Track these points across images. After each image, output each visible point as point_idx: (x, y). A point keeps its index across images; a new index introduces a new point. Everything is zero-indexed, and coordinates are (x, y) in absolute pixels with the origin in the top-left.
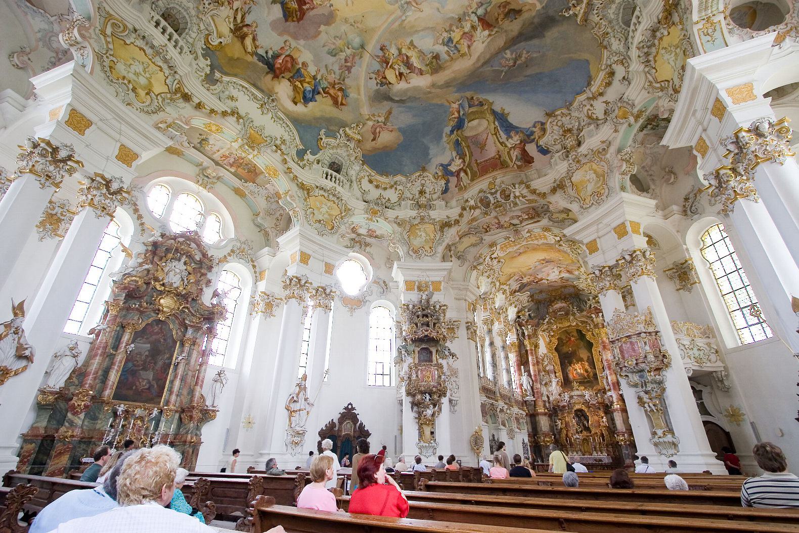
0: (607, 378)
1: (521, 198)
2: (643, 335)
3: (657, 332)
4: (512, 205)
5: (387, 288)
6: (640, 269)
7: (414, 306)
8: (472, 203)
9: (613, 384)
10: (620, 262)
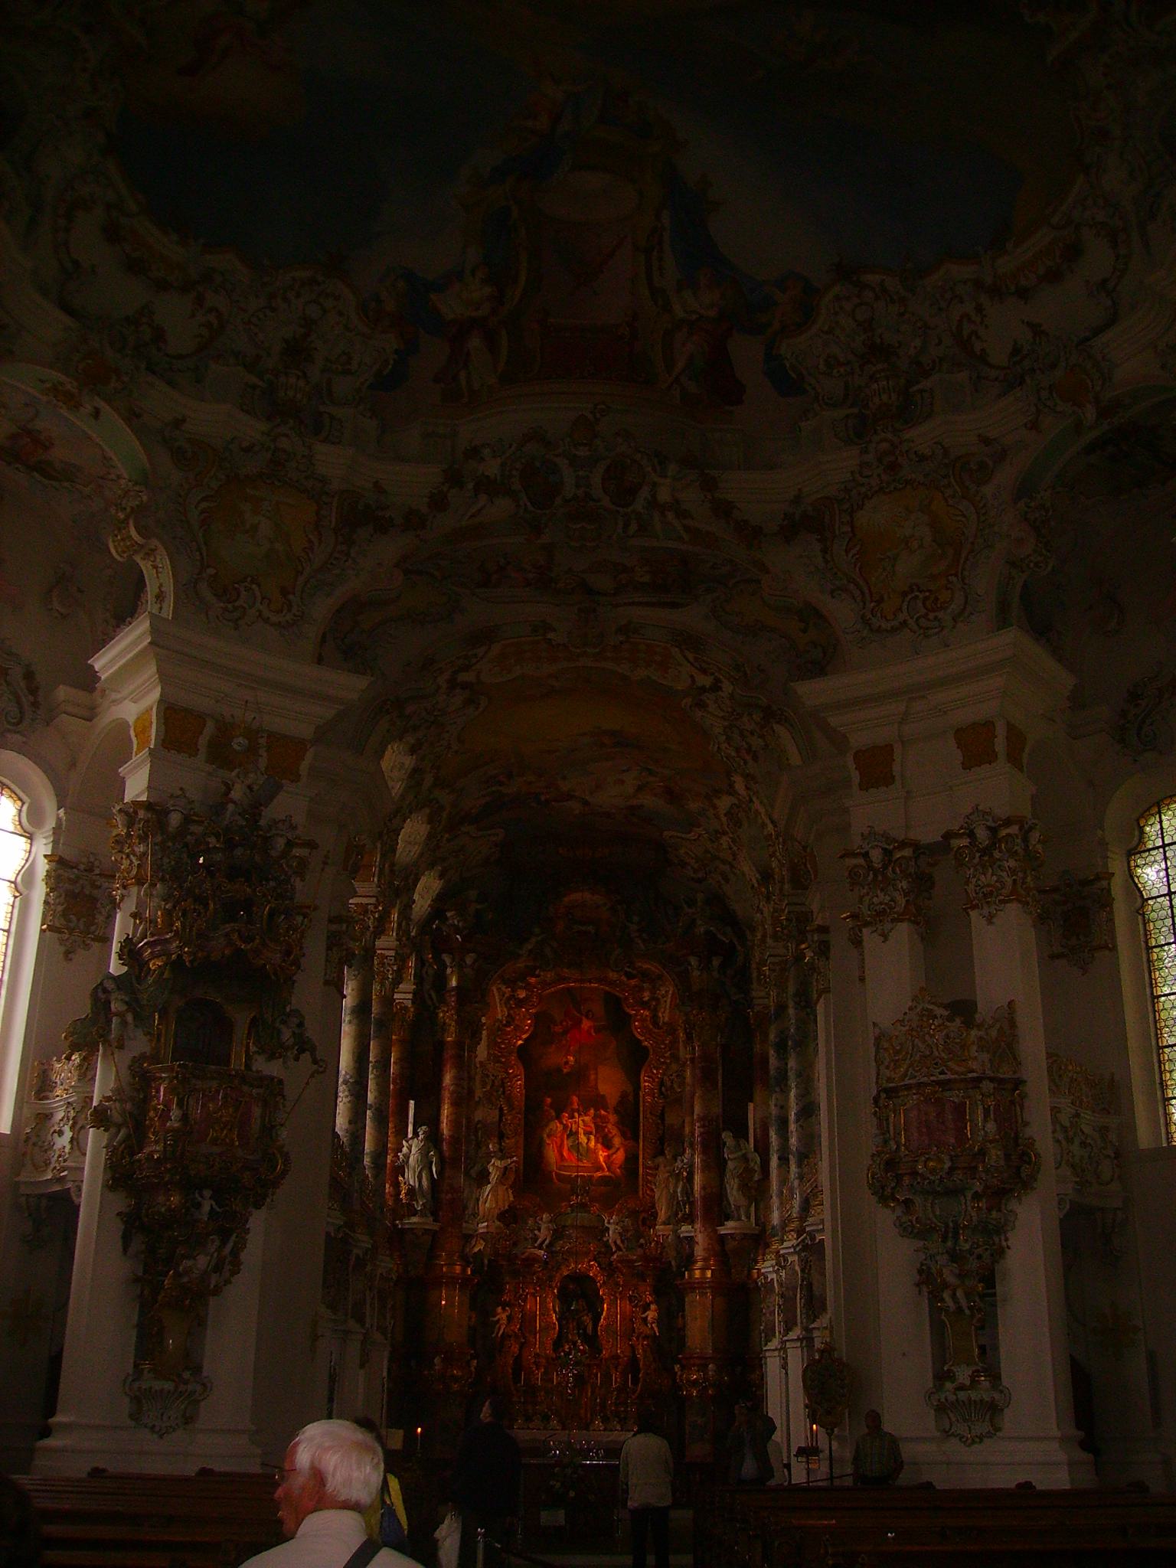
0: (690, 1179)
1: (670, 515)
2: (987, 1086)
3: (1018, 1083)
4: (633, 528)
5: (35, 705)
6: (1009, 881)
7: (187, 820)
8: (492, 468)
10: (956, 843)
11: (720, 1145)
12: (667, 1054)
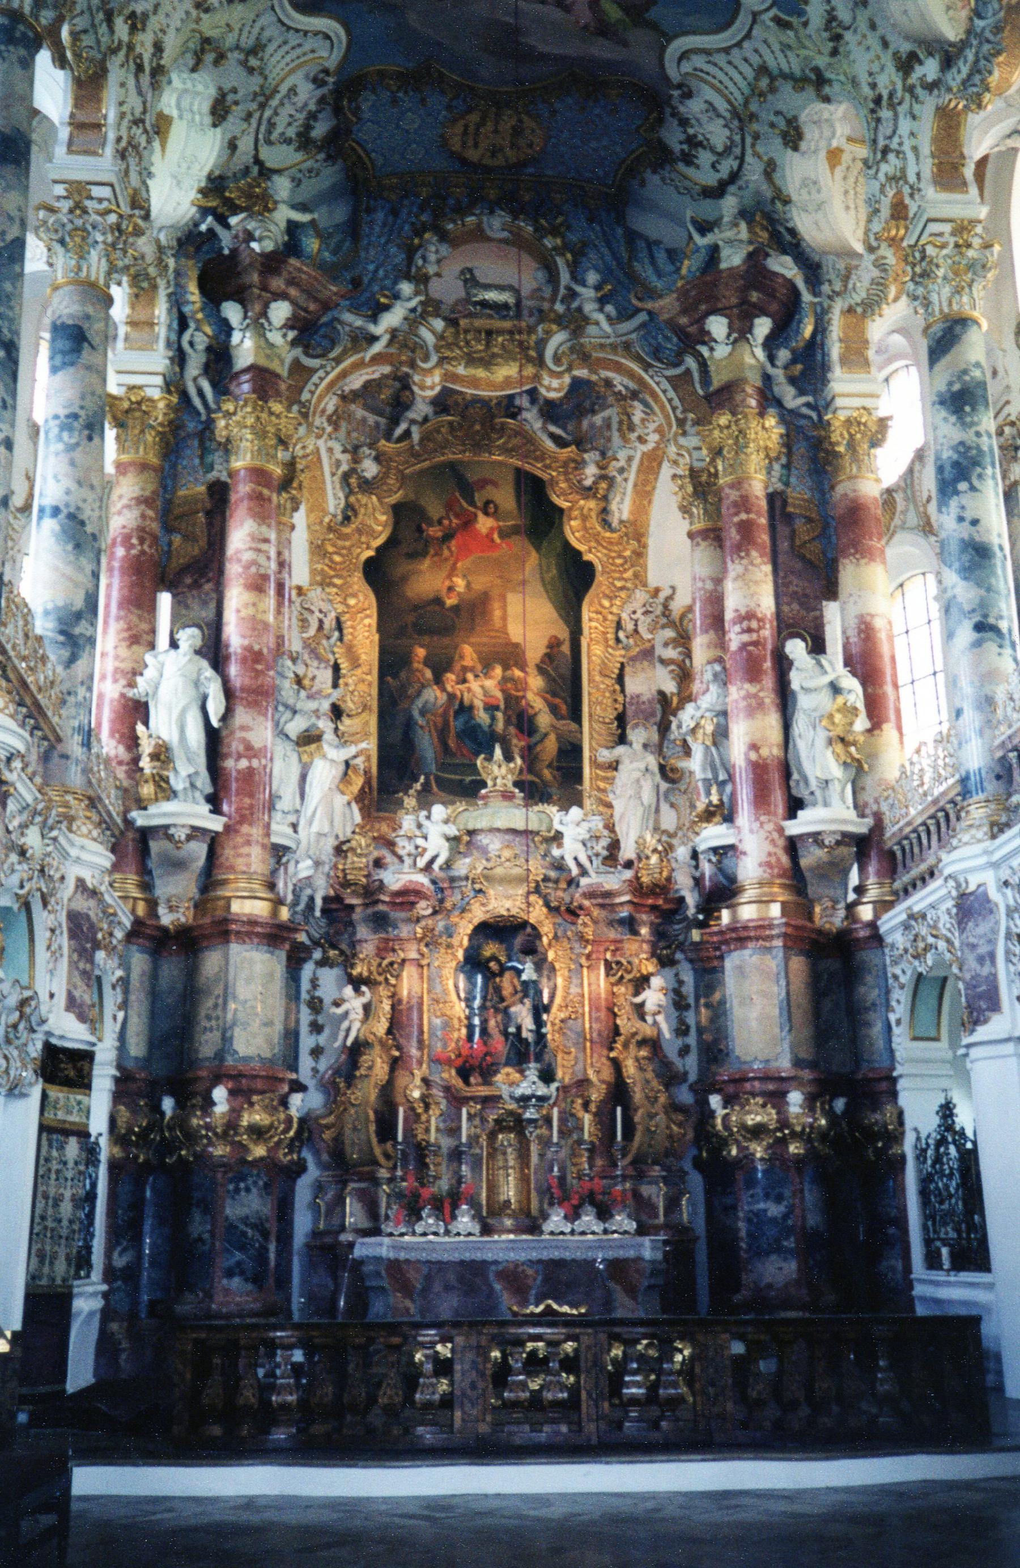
0: (721, 734)
9: (759, 770)
11: (783, 665)
12: (628, 574)
